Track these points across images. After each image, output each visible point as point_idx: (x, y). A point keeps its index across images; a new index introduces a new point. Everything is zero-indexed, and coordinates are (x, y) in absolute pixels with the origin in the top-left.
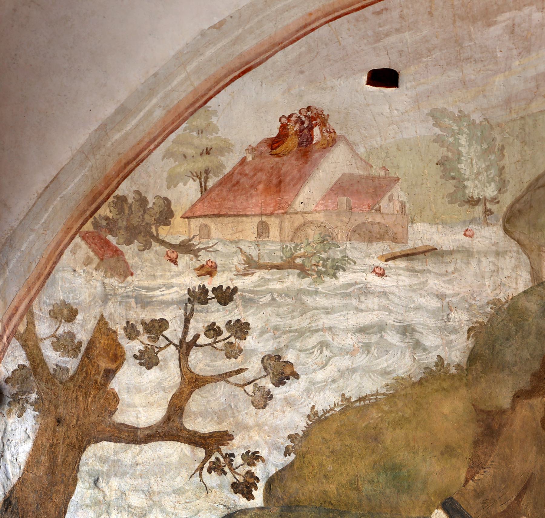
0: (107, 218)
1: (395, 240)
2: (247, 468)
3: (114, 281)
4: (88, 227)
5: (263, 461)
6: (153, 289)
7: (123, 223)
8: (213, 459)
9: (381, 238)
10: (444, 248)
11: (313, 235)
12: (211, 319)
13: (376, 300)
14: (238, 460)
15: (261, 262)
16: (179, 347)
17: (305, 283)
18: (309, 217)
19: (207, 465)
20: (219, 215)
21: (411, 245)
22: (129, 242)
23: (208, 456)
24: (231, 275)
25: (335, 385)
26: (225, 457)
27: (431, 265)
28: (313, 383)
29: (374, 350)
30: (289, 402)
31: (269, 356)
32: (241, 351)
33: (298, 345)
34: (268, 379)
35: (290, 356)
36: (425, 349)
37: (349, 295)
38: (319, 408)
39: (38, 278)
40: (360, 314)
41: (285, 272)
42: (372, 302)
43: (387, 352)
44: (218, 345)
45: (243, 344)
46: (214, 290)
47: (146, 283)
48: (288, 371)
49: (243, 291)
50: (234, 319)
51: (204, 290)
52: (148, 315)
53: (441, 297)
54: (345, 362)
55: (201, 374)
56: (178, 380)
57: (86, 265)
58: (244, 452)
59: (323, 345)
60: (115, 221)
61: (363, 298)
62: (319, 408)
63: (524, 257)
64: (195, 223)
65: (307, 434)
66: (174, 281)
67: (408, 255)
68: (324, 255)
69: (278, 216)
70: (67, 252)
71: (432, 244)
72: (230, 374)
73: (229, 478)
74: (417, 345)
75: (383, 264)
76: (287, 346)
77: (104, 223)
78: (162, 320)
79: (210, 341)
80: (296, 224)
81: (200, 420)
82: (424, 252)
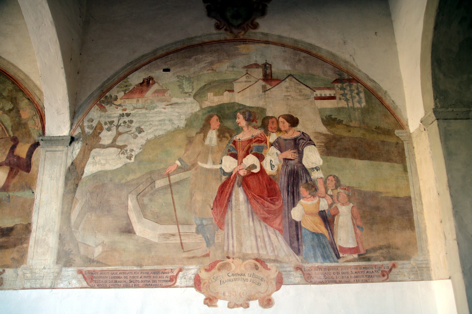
0: (103, 100)
1: (168, 101)
2: (131, 153)
3: (103, 113)
4: (98, 102)
5: (134, 151)
6: (112, 114)
7: (106, 101)
8: (122, 151)
9: (165, 101)
10: (180, 103)
11: (149, 101)
12: (124, 120)
13: (163, 114)
14: (128, 151)
15: (137, 107)
16: (116, 126)
17: (147, 111)
18: (148, 98)
19: (121, 153)
20: (128, 98)
21: (172, 102)
22: (107, 105)
23: (121, 150)
24: (130, 110)
25: (153, 133)
26: (125, 151)
27: (176, 106)
28: (147, 133)
29: (162, 125)
30: (142, 137)
31: (138, 127)
32: (131, 126)
33: (144, 124)
34: (137, 132)
35: (142, 127)
36: (175, 124)
37: (157, 113)
38: (149, 138)
39: (86, 113)
40: (160, 117)
41: (142, 109)
42: (162, 115)
43: (166, 125)
44: (126, 125)
45: (131, 125)
46: (126, 114)
47: (110, 113)
48: (142, 130)
49: (133, 114)
50: (130, 120)
51: (123, 114)
52: (110, 120)
53: (178, 113)
54: (156, 128)
55: (121, 132)
56: (115, 133)
57: (97, 110)
58: (130, 149)
59: (150, 124)
60: (104, 101)
61: (160, 114)
62: (149, 138)
63: (198, 103)
64: (122, 100)
65: (145, 144)
66: (117, 112)
67: (171, 105)
68: (151, 105)
69: (142, 98)
70: (93, 108)
71: (177, 102)
72: (128, 132)
73: (126, 155)
74: (173, 123)
75: (165, 107)
76: (142, 125)
77: (102, 101)
78: (113, 121)
79: (124, 125)
80: (145, 99)
81: (120, 142)
82: (175, 104)
